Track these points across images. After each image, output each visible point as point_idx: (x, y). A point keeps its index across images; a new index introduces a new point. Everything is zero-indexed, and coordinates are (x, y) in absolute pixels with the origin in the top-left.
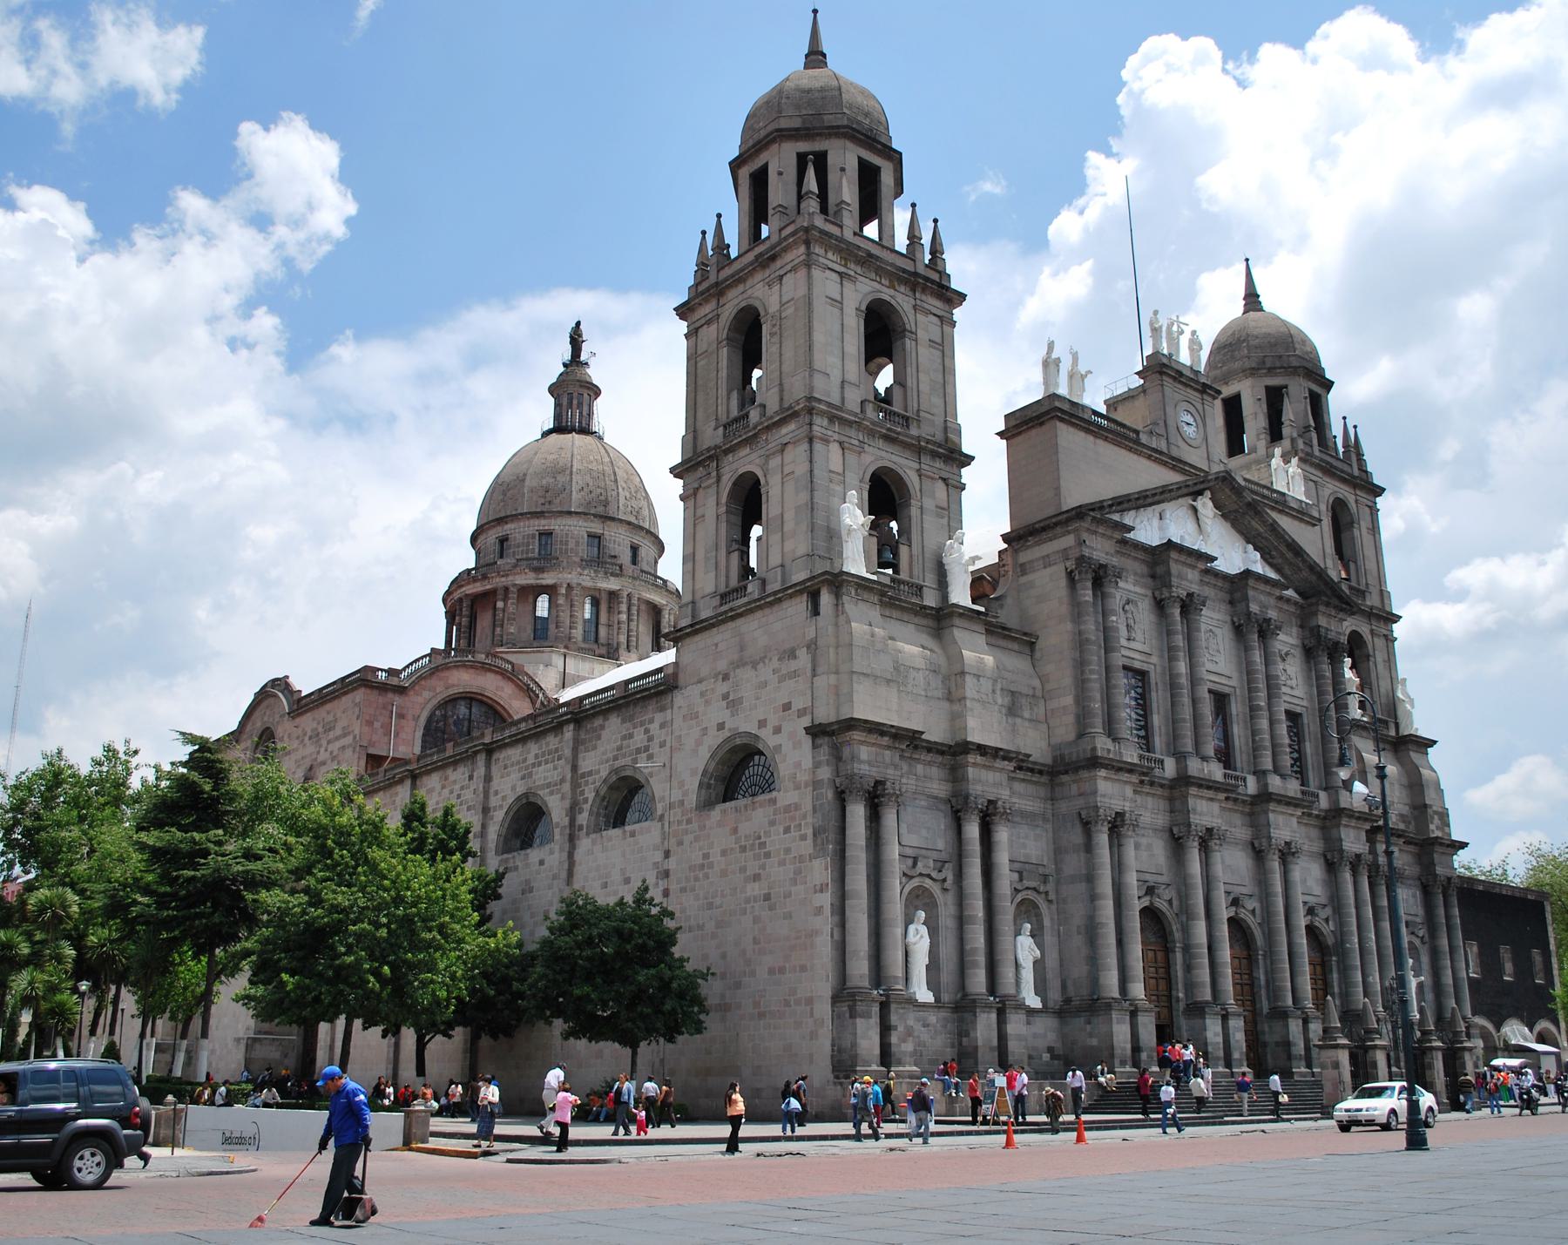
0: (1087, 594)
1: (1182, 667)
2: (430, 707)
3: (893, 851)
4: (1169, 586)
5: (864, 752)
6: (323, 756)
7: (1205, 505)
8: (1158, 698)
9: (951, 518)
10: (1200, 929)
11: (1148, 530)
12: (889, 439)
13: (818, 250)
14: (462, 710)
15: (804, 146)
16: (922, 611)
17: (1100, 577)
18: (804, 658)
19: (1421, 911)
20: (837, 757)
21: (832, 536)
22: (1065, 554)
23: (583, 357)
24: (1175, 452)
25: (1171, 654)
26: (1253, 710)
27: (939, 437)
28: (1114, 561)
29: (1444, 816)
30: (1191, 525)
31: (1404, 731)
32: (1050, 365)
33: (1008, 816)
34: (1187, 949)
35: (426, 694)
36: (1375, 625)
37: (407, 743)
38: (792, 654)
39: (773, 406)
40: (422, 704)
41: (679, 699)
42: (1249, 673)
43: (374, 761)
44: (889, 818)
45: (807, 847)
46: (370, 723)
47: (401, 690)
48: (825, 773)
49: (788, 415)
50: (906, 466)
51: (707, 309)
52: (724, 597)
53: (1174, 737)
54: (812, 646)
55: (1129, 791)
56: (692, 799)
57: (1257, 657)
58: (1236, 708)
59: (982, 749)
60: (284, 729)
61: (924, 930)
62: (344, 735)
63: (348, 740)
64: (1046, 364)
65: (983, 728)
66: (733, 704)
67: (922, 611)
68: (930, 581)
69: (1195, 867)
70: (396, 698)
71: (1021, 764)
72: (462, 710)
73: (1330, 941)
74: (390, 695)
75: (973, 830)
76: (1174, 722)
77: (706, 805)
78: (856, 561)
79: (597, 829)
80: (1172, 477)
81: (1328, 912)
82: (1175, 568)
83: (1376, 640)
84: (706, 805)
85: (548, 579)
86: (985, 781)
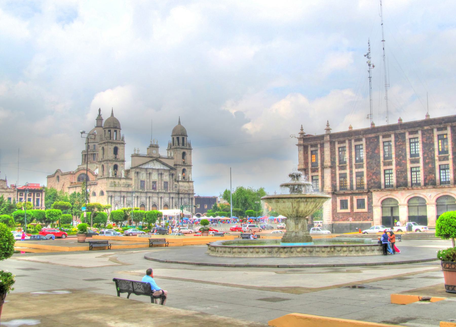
0: (136, 175)
1: (148, 180)
2: (78, 176)
3: (113, 201)
4: (147, 172)
5: (110, 193)
6: (66, 181)
7: (155, 162)
8: (146, 183)
9: (123, 167)
10: (148, 206)
11: (146, 166)
12: (116, 161)
13: (108, 143)
14: (82, 175)
15: (109, 129)
16: (119, 178)
17: (138, 173)
18: (106, 184)
19: (188, 201)
20: (108, 193)
21: (109, 173)
22: (134, 171)
23: (101, 114)
24: (151, 156)
25: (147, 179)
26: (159, 183)
27: (122, 159)
28: (140, 171)
29: (193, 190)
30: (153, 164)
31: (190, 180)
32: (135, 150)
33: (126, 197)
34: (146, 208)
35: (77, 174)
36: (188, 167)
37: (75, 180)
38: (105, 184)
39: (105, 159)
40: (77, 175)
41: (98, 185)
42: (159, 178)
43: (72, 183)
44: (113, 198)
45: (106, 201)
46: (71, 178)
47: (74, 174)
48: (107, 195)
49: (105, 161)
50: (118, 164)
51: (100, 145)
52: (101, 176)
53: (147, 188)
54: (107, 183)
55: (139, 194)
56: (99, 195)
57: (160, 177)
58: (157, 183)
59: (123, 191)
60: (60, 177)
61: (117, 207)
62: (68, 180)
63: (68, 180)
64: (134, 150)
65: (123, 189)
66: (101, 187)
67: (119, 178)
68: (120, 174)
69: (148, 200)
70: (74, 175)
71: (127, 192)
72: (82, 175)
73: (169, 206)
74: (73, 175)
75: (122, 199)
76: (147, 186)
77: (100, 196)
78: (111, 176)
79: (92, 196)
80: (151, 159)
81: (169, 203)
82: (148, 170)
83: (188, 169)
84: (100, 196)
85: (95, 153)
86: (123, 194)
